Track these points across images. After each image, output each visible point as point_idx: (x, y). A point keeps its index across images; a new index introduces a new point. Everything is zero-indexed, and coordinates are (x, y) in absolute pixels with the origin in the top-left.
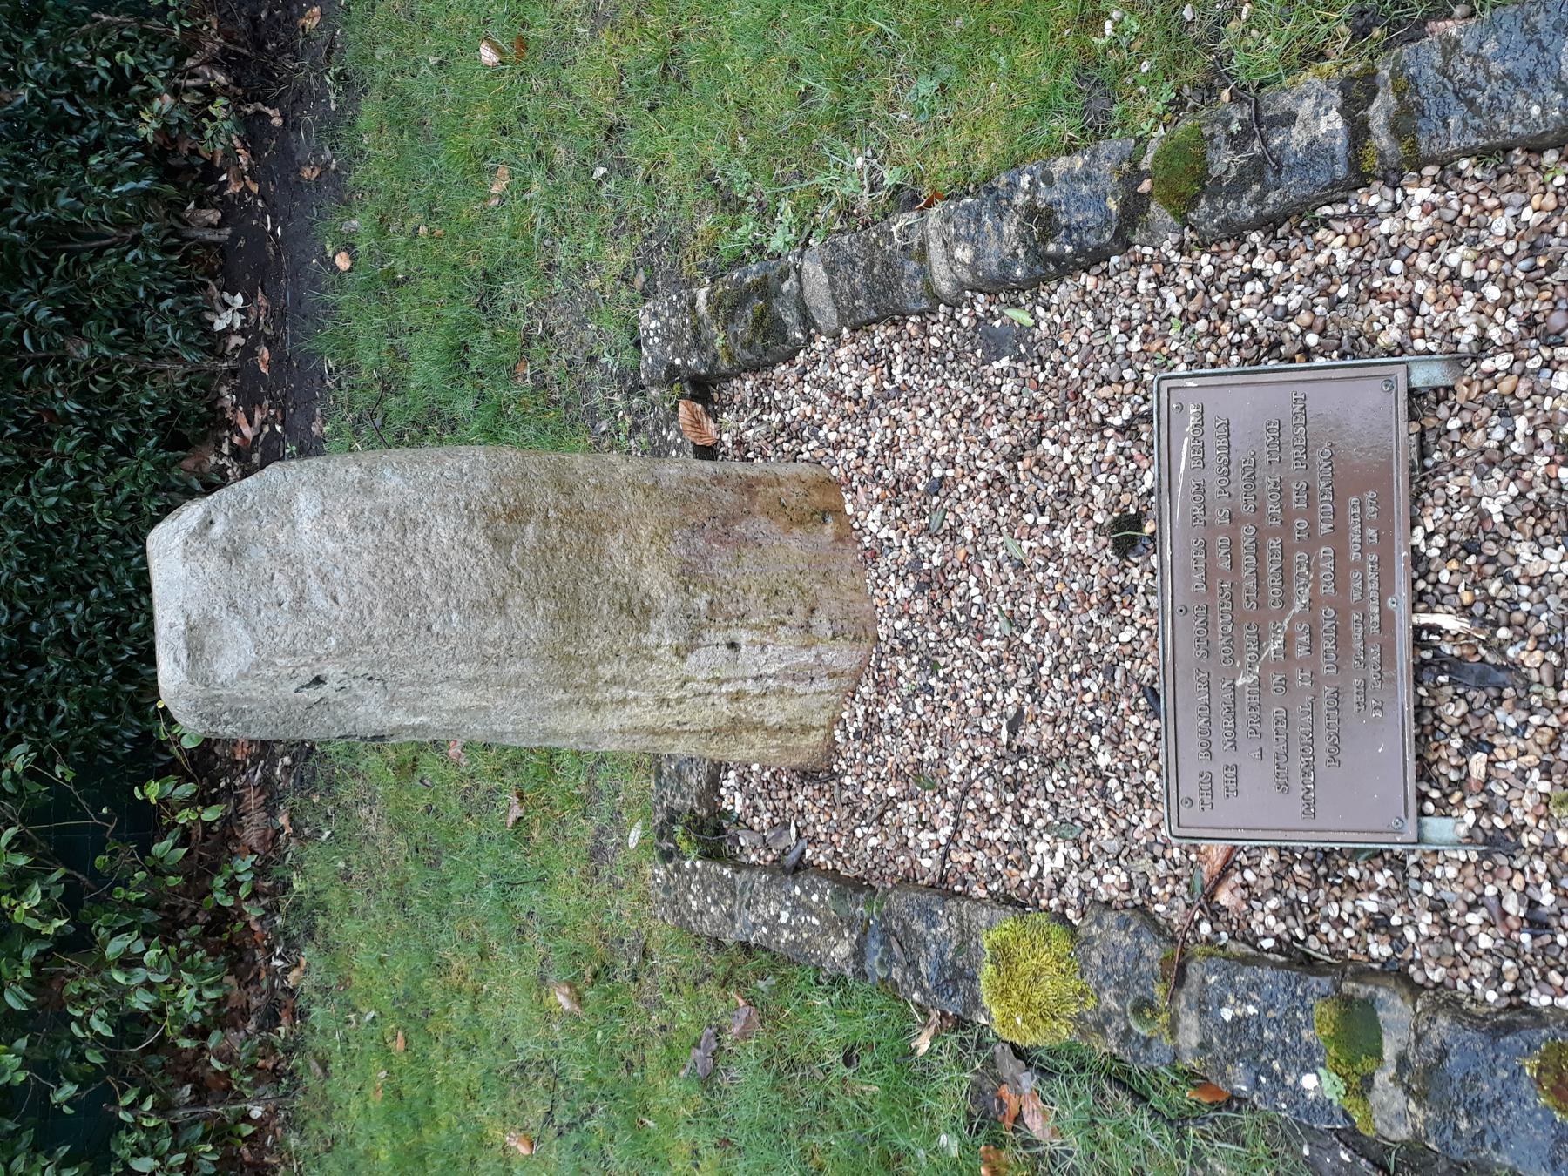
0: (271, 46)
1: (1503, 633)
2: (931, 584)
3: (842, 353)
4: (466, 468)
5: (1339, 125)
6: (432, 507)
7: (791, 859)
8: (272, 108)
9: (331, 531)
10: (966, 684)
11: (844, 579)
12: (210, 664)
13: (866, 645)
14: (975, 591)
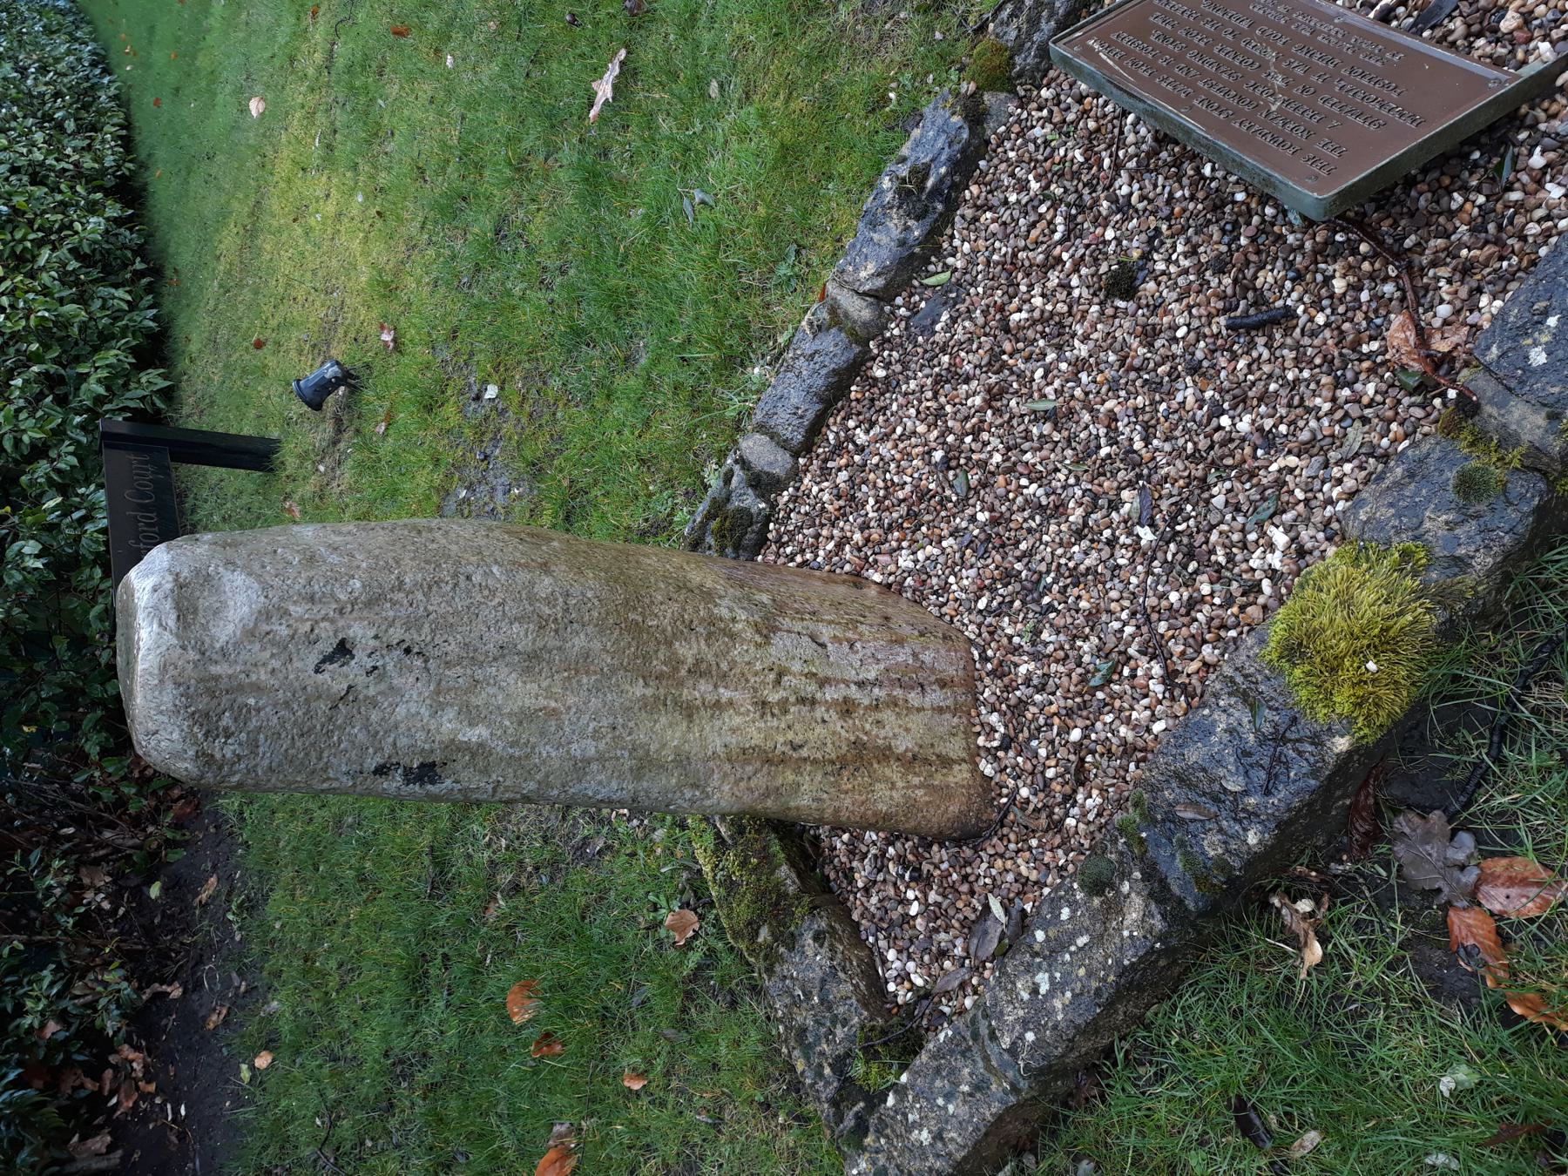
8: (170, 985)
12: (205, 628)
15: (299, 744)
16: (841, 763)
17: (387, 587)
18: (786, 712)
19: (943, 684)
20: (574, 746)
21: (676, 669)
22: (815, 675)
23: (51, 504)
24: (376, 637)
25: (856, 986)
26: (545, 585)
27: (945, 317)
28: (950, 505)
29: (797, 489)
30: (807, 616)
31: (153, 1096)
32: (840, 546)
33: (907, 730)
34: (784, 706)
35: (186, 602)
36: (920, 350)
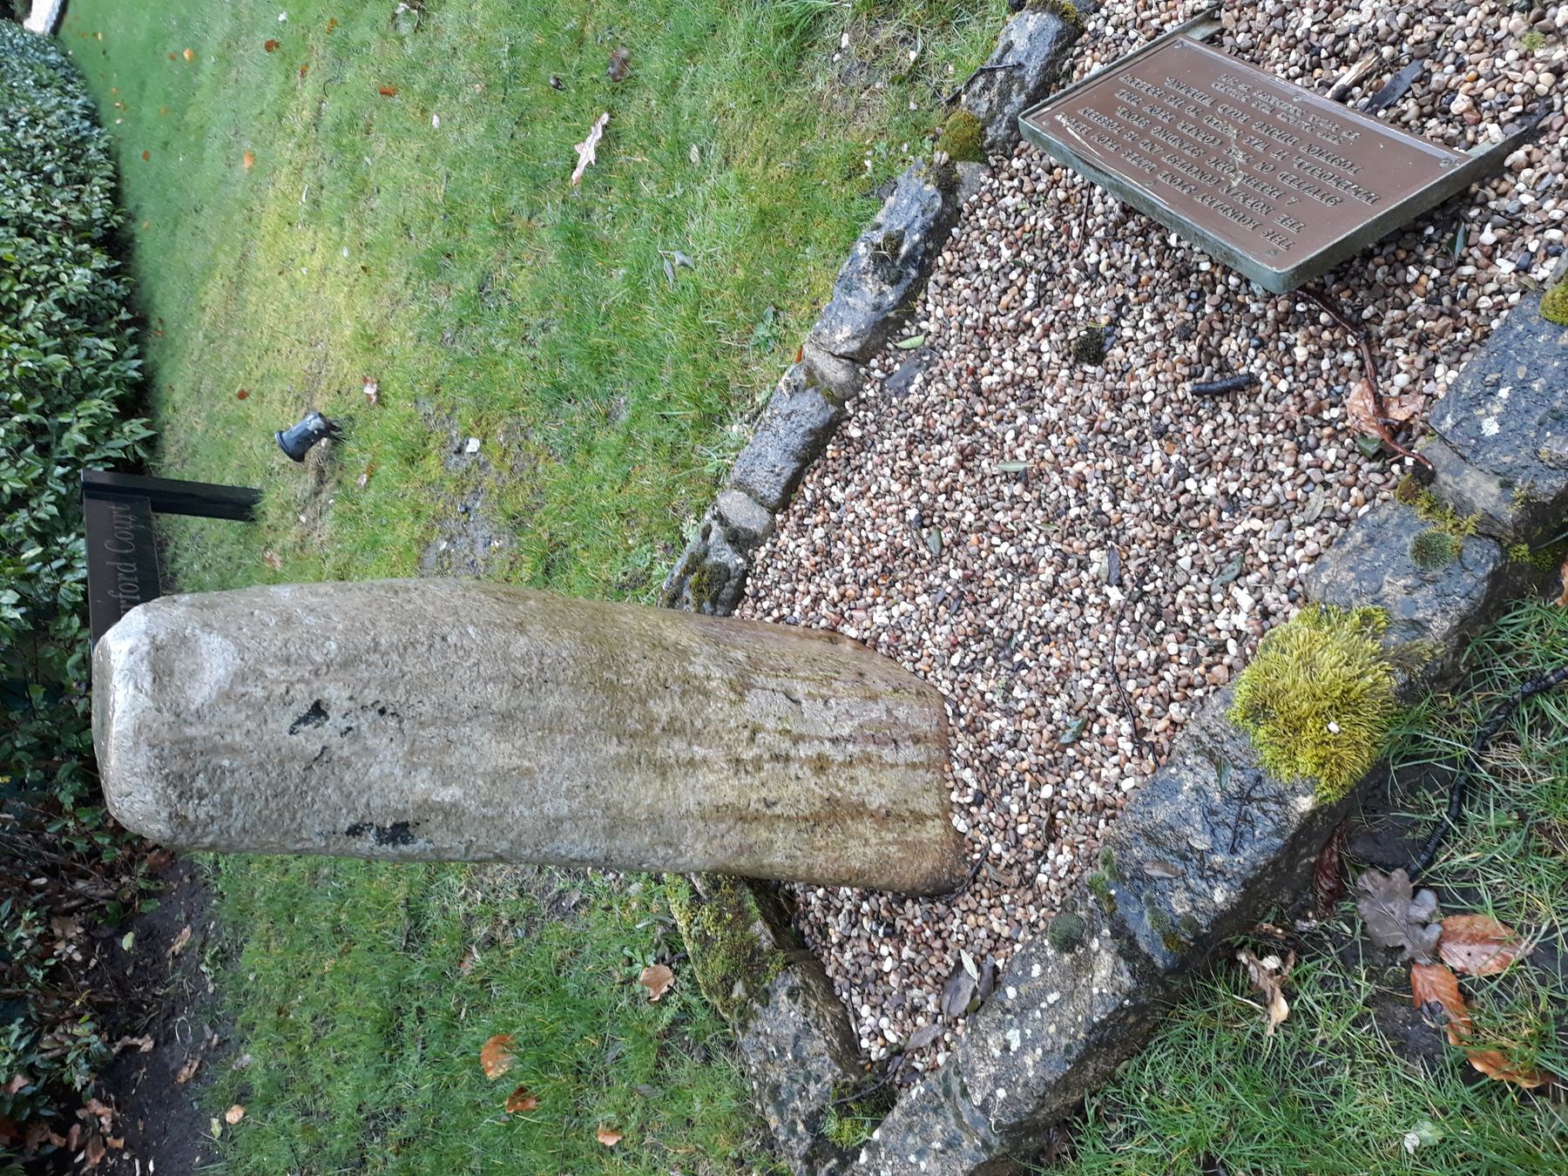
8: (141, 1037)
12: (181, 690)
15: (273, 805)
16: (816, 820)
17: (363, 648)
18: (760, 769)
19: (917, 740)
20: (547, 805)
21: (650, 728)
22: (789, 732)
23: (31, 554)
24: (351, 698)
25: (830, 1043)
26: (520, 645)
27: (919, 379)
28: (924, 562)
29: (775, 545)
30: (782, 673)
31: (121, 1151)
32: (816, 601)
33: (881, 786)
34: (758, 764)
35: (162, 664)
36: (894, 411)
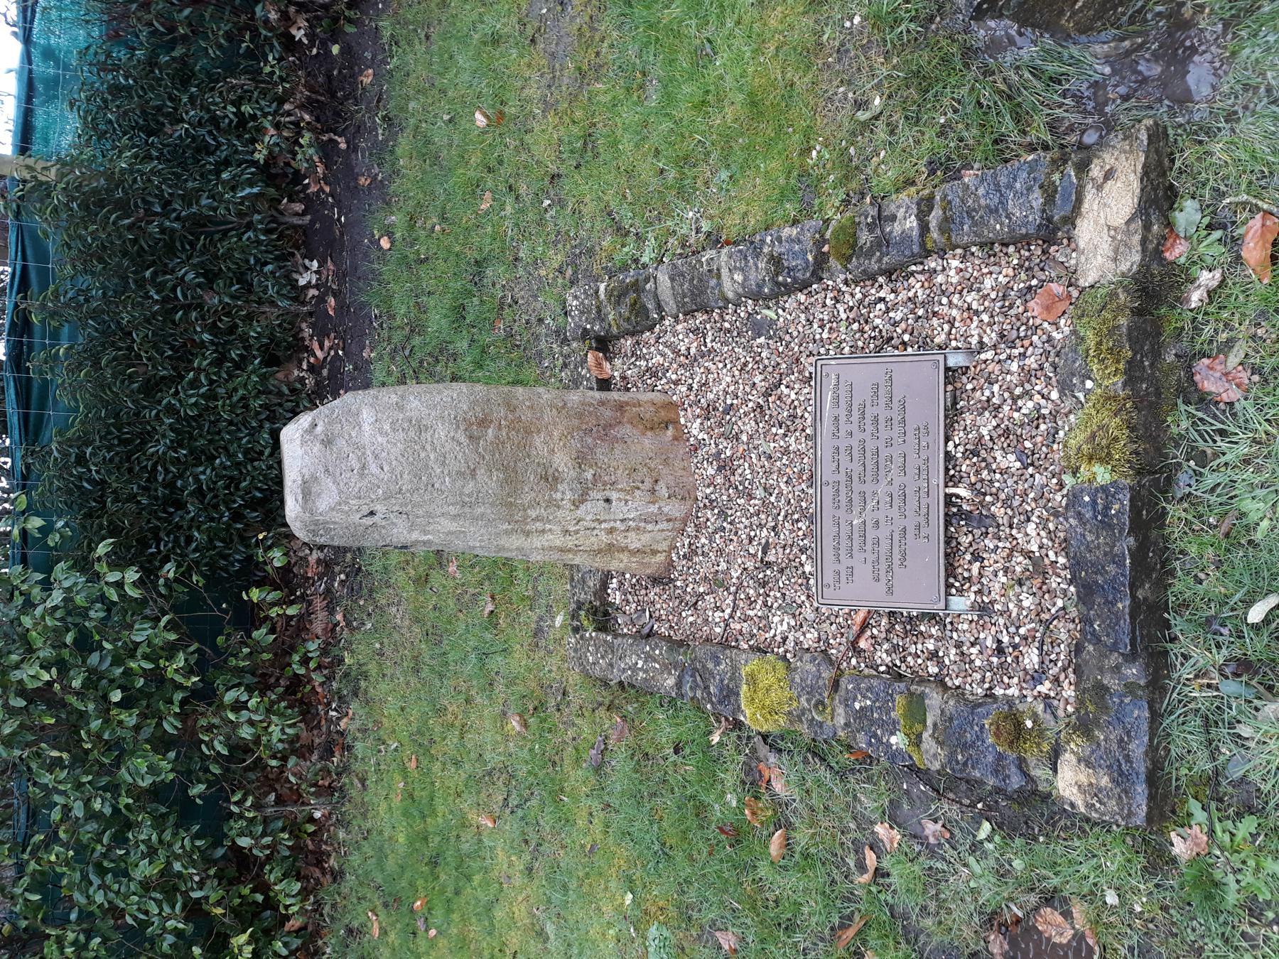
0: (340, 94)
1: (988, 498)
2: (725, 466)
3: (679, 327)
4: (456, 397)
5: (915, 224)
6: (436, 418)
7: (646, 630)
9: (381, 431)
10: (742, 526)
11: (678, 464)
13: (689, 503)
14: (748, 471)
